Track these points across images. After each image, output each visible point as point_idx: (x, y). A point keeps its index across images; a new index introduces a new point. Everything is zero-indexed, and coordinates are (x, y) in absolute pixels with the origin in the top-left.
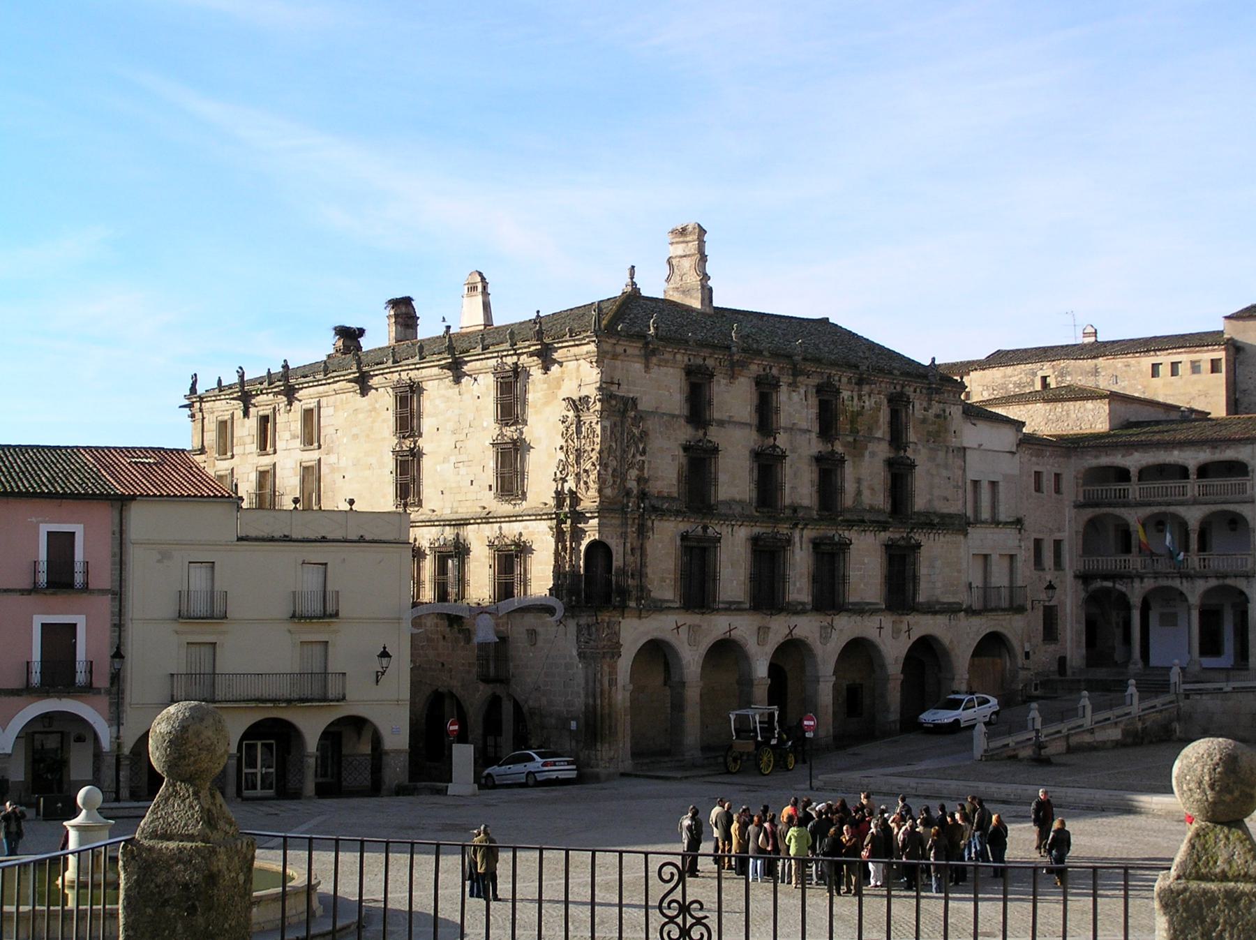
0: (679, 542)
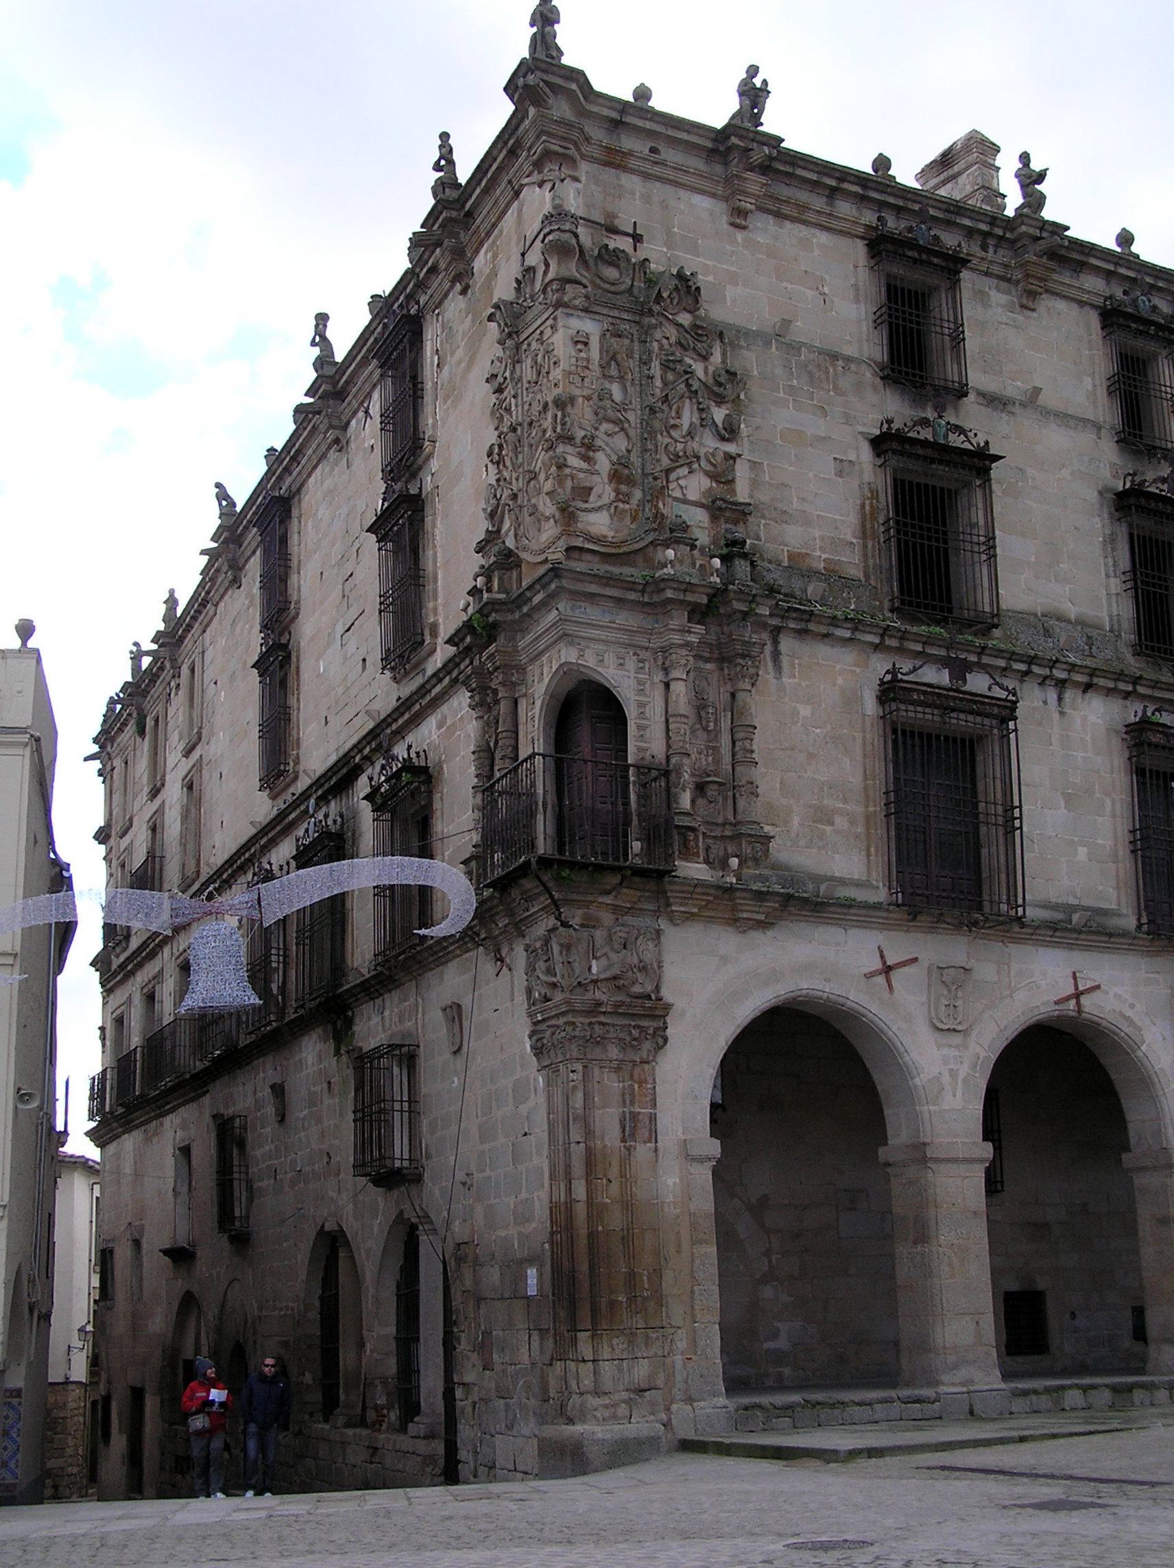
0: (870, 706)
